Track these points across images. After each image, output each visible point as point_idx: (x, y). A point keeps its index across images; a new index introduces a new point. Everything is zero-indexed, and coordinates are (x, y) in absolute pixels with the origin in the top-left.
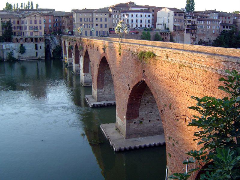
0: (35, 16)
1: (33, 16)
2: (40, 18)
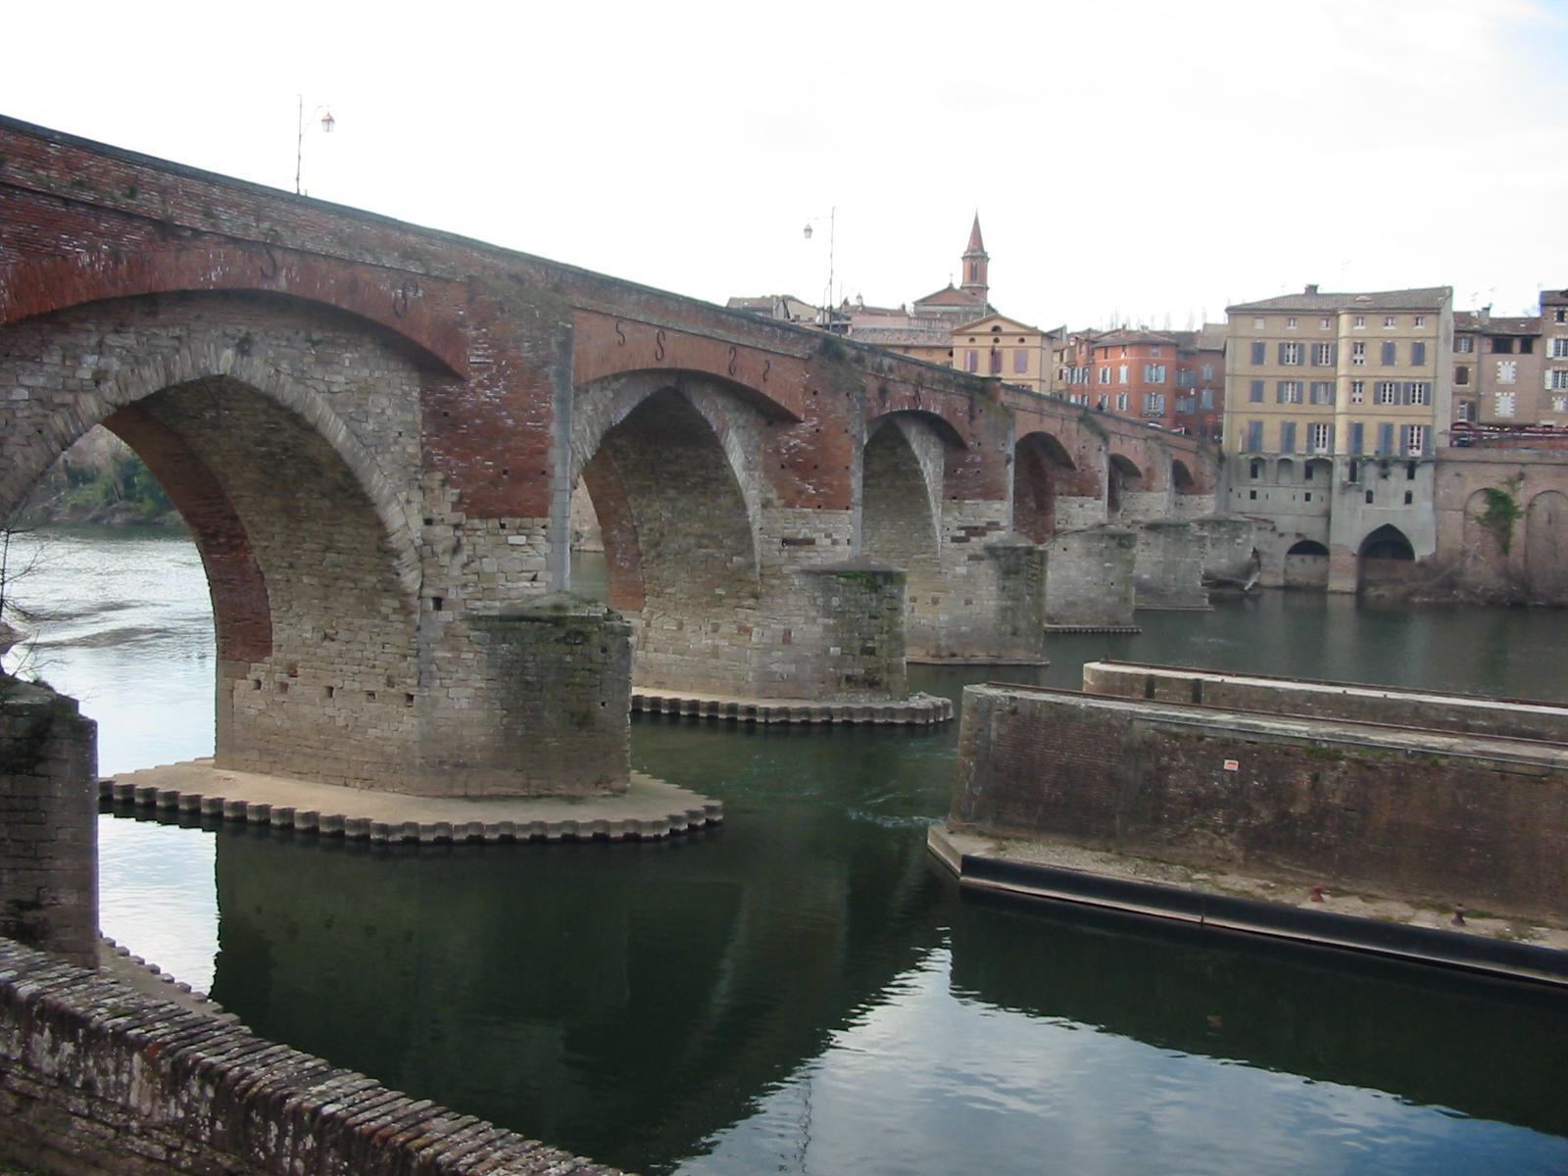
0: (996, 329)
1: (987, 328)
2: (1022, 340)
